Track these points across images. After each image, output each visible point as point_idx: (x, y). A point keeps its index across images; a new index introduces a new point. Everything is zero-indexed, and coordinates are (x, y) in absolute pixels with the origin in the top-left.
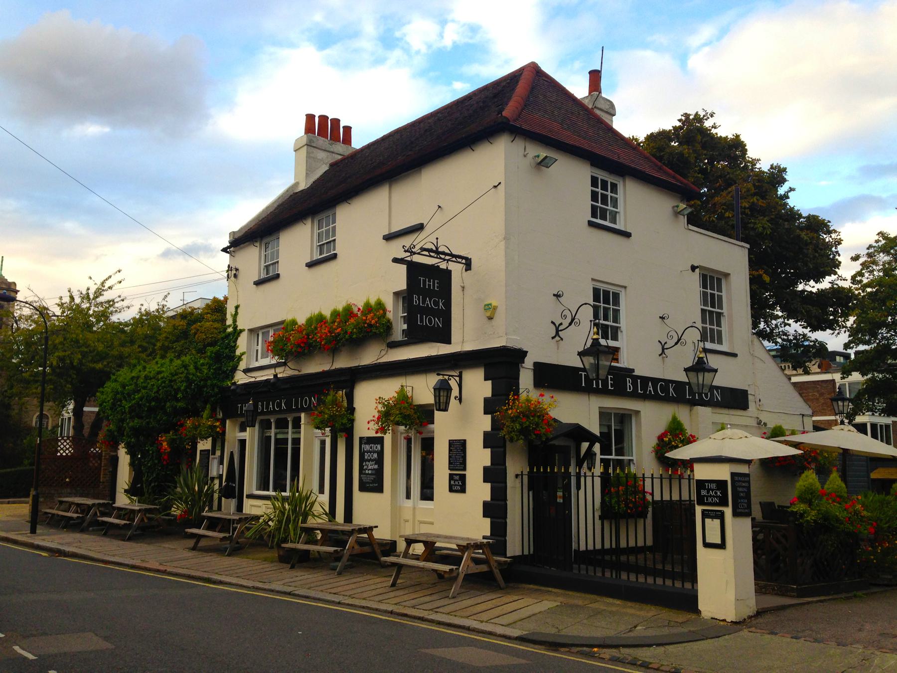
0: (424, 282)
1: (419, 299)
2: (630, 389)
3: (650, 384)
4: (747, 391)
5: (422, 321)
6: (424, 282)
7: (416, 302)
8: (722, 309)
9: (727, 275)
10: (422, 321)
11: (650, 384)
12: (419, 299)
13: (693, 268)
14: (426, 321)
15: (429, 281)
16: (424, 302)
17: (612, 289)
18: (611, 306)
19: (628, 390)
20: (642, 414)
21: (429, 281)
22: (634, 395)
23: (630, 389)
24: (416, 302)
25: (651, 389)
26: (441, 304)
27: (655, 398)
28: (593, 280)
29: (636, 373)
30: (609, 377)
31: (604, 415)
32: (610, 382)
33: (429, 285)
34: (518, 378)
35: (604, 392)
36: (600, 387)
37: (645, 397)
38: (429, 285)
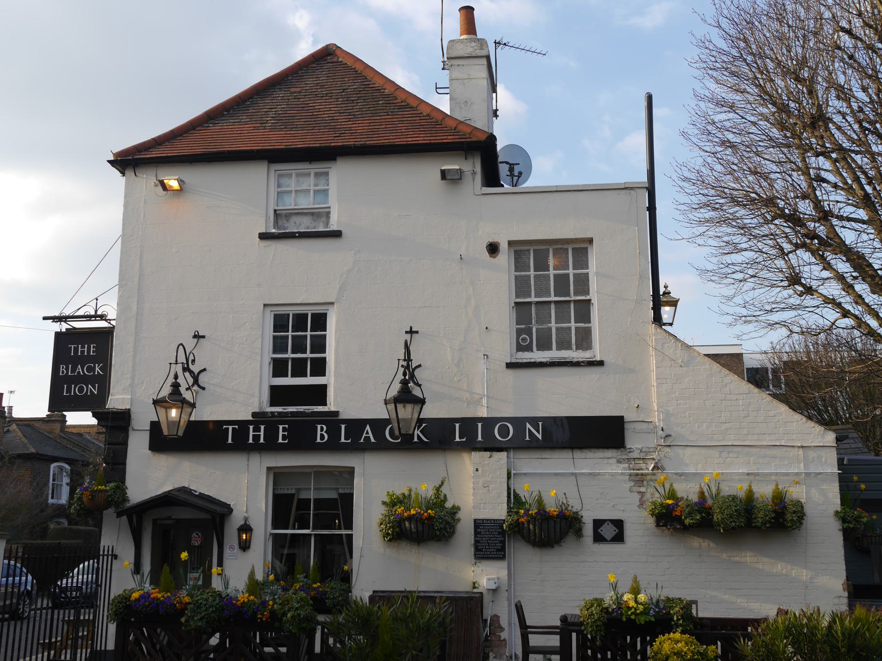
0: (76, 349)
1: (67, 369)
2: (322, 437)
3: (368, 428)
4: (622, 417)
5: (69, 390)
6: (76, 349)
7: (63, 372)
8: (587, 292)
9: (590, 241)
10: (69, 390)
11: (368, 428)
12: (67, 369)
13: (493, 249)
14: (75, 390)
15: (83, 347)
16: (73, 371)
17: (310, 311)
18: (309, 333)
19: (318, 440)
20: (357, 472)
21: (83, 347)
22: (332, 446)
23: (322, 437)
24: (63, 372)
25: (371, 435)
26: (97, 369)
27: (381, 446)
28: (265, 305)
29: (342, 416)
30: (281, 427)
31: (277, 475)
32: (281, 433)
33: (83, 352)
34: (125, 444)
35: (270, 446)
36: (262, 441)
37: (357, 447)
38: (83, 352)
